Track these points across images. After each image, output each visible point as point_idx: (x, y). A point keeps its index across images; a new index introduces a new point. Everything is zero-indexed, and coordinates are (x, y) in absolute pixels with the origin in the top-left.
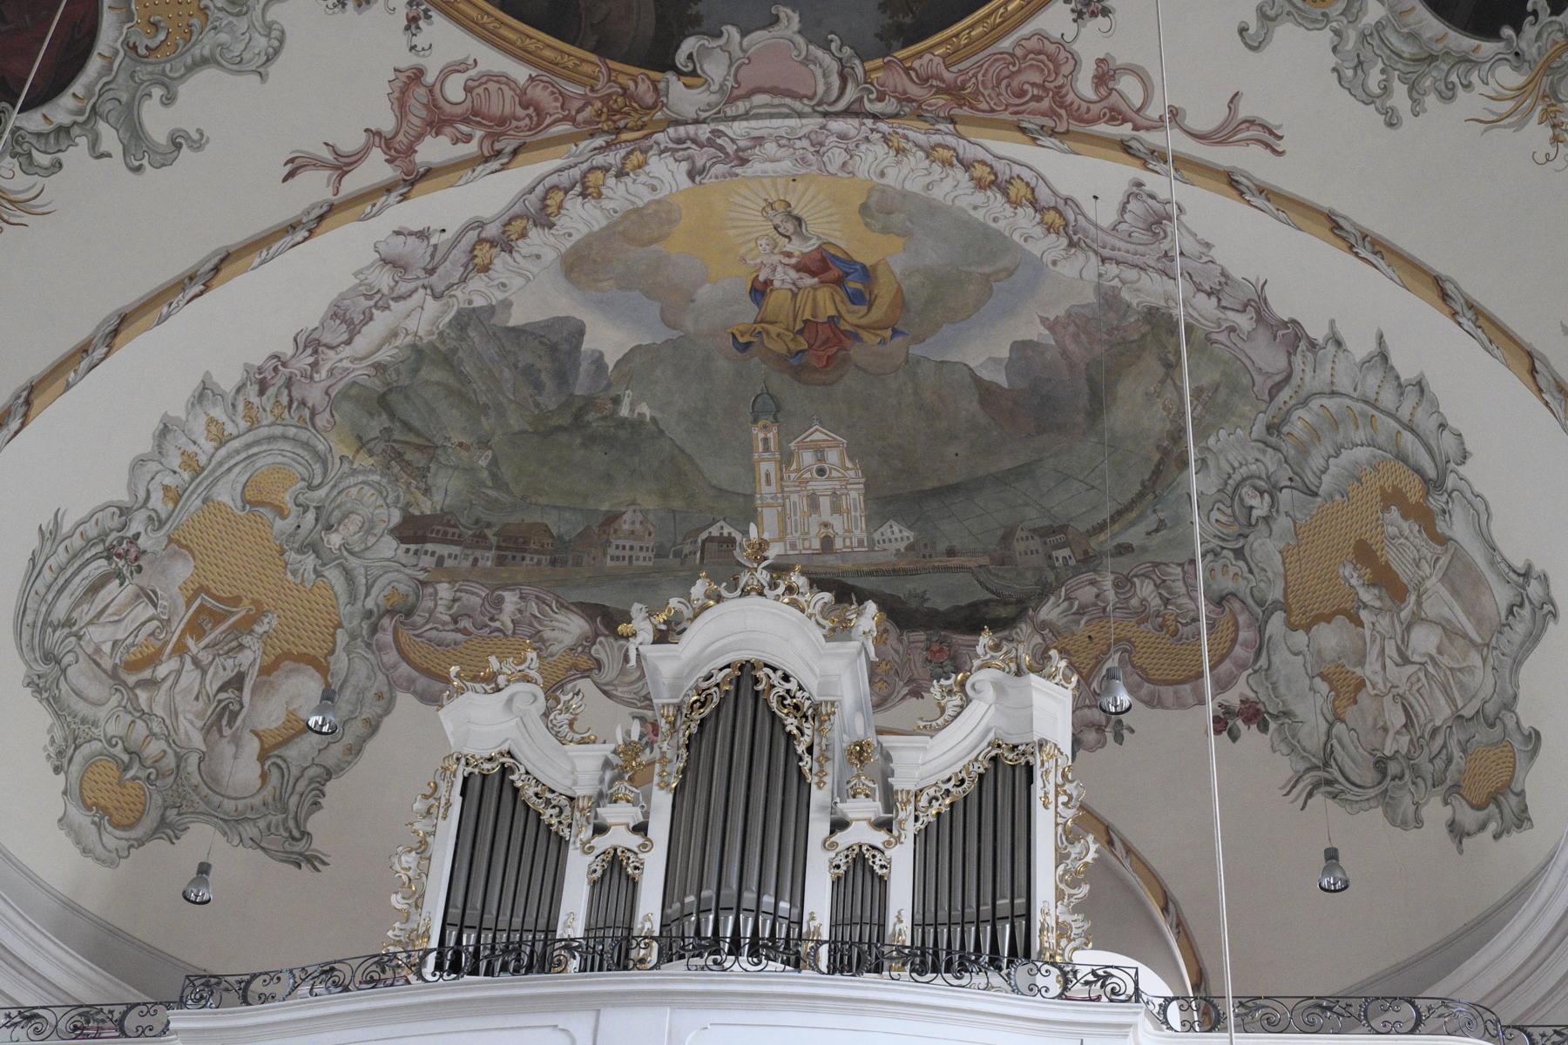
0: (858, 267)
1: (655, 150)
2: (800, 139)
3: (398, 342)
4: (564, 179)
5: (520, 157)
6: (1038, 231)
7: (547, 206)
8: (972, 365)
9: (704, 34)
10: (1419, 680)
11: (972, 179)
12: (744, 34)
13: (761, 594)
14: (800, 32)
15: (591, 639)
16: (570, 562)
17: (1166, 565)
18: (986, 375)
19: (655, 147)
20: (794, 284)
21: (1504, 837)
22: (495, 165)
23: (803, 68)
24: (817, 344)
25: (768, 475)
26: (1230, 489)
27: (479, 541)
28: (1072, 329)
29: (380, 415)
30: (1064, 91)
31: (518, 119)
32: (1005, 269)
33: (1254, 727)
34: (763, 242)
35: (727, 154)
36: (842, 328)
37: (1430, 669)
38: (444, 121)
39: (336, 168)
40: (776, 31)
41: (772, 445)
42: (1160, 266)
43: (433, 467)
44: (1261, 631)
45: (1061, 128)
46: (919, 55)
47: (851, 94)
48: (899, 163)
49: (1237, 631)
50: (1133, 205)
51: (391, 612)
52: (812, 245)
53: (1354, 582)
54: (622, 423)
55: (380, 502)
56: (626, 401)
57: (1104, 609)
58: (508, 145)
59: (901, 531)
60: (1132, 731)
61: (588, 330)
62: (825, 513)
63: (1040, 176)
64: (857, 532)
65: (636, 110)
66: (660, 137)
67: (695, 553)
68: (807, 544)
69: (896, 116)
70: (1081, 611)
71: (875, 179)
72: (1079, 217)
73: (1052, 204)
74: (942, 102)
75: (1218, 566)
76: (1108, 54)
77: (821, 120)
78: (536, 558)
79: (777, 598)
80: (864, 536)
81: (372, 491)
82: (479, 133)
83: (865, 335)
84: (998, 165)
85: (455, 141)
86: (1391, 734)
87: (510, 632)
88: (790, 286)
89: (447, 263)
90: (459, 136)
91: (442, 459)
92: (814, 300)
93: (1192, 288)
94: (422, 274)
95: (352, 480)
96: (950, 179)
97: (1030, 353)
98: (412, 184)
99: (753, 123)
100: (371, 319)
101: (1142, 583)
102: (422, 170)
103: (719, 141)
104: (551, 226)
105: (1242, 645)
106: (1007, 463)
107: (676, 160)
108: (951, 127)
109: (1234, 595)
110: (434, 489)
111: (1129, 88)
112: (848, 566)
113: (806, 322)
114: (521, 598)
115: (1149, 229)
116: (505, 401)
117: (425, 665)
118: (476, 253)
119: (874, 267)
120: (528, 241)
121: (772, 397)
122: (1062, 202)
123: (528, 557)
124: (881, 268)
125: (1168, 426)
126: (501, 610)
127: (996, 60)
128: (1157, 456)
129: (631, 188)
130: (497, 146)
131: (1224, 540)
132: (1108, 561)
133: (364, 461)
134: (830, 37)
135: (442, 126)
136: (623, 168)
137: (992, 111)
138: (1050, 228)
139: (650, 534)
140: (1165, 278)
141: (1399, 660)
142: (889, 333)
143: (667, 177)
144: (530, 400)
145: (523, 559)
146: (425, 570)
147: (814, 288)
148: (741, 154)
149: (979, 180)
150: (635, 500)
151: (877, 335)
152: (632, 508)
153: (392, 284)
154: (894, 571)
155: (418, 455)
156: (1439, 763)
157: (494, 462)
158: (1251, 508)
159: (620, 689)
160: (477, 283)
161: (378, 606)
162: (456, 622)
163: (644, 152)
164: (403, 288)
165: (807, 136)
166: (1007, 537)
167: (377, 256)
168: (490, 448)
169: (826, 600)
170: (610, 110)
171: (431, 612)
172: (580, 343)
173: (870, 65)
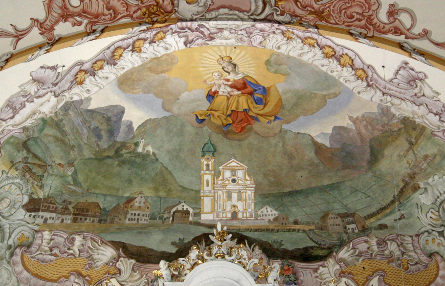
0: (261, 88)
1: (170, 32)
2: (241, 30)
3: (36, 117)
4: (124, 44)
5: (105, 34)
6: (353, 78)
7: (114, 55)
8: (313, 135)
11: (323, 53)
13: (223, 258)
16: (108, 221)
17: (404, 236)
18: (319, 140)
19: (170, 31)
20: (229, 93)
22: (92, 37)
24: (237, 121)
25: (207, 182)
26: (438, 203)
27: (65, 211)
28: (364, 123)
29: (23, 151)
30: (372, 17)
31: (105, 15)
32: (335, 93)
34: (216, 74)
39: (16, 36)
42: (412, 99)
43: (46, 175)
45: (370, 35)
47: (268, 11)
48: (288, 43)
50: (402, 72)
51: (20, 246)
52: (240, 76)
54: (139, 155)
55: (19, 192)
56: (141, 145)
57: (372, 255)
58: (100, 27)
59: (271, 211)
61: (126, 111)
63: (357, 55)
64: (250, 210)
65: (162, 13)
66: (173, 26)
67: (169, 218)
68: (224, 215)
69: (289, 23)
70: (360, 255)
71: (275, 50)
72: (374, 75)
73: (361, 67)
74: (312, 18)
75: (430, 239)
76: (395, 2)
77: (252, 23)
78: (92, 219)
79: (232, 261)
80: (253, 212)
81: (16, 187)
82: (85, 21)
83: (261, 118)
84: (337, 49)
85: (74, 25)
87: (77, 256)
88: (227, 94)
89: (63, 81)
90: (76, 22)
91: (51, 172)
92: (238, 101)
93: (427, 111)
94: (51, 86)
95: (7, 182)
96: (312, 53)
97: (342, 132)
98: (52, 45)
99: (219, 22)
100: (24, 107)
101: (391, 243)
102: (57, 38)
103: (201, 29)
104: (115, 64)
105: (440, 277)
106: (326, 182)
107: (179, 37)
108: (316, 30)
109: (437, 253)
110: (45, 186)
111: (405, 19)
112: (245, 226)
113: (233, 111)
114: (84, 238)
115: (409, 83)
116: (82, 143)
117: (36, 272)
118: (78, 76)
119: (269, 88)
120: (103, 71)
121: (213, 145)
122: (367, 67)
123: (88, 218)
125: (409, 171)
126: (73, 245)
128: (402, 185)
129: (156, 48)
130: (94, 28)
132: (373, 231)
133: (13, 173)
135: (68, 18)
136: (153, 39)
137: (337, 24)
138: (358, 78)
139: (148, 208)
140: (414, 105)
142: (273, 118)
143: (174, 44)
144: (95, 143)
145: (86, 219)
146: (37, 225)
147: (238, 96)
148: (211, 35)
149: (327, 54)
150: (142, 192)
151: (268, 119)
152: (140, 196)
153: (36, 90)
154: (267, 230)
155: (39, 169)
157: (75, 172)
160: (76, 90)
161: (14, 242)
162: (51, 250)
163: (165, 33)
164: (41, 92)
165: (244, 29)
166: (325, 216)
167: (31, 78)
168: (73, 166)
169: (255, 262)
170: (150, 12)
171: (40, 246)
172: (122, 117)
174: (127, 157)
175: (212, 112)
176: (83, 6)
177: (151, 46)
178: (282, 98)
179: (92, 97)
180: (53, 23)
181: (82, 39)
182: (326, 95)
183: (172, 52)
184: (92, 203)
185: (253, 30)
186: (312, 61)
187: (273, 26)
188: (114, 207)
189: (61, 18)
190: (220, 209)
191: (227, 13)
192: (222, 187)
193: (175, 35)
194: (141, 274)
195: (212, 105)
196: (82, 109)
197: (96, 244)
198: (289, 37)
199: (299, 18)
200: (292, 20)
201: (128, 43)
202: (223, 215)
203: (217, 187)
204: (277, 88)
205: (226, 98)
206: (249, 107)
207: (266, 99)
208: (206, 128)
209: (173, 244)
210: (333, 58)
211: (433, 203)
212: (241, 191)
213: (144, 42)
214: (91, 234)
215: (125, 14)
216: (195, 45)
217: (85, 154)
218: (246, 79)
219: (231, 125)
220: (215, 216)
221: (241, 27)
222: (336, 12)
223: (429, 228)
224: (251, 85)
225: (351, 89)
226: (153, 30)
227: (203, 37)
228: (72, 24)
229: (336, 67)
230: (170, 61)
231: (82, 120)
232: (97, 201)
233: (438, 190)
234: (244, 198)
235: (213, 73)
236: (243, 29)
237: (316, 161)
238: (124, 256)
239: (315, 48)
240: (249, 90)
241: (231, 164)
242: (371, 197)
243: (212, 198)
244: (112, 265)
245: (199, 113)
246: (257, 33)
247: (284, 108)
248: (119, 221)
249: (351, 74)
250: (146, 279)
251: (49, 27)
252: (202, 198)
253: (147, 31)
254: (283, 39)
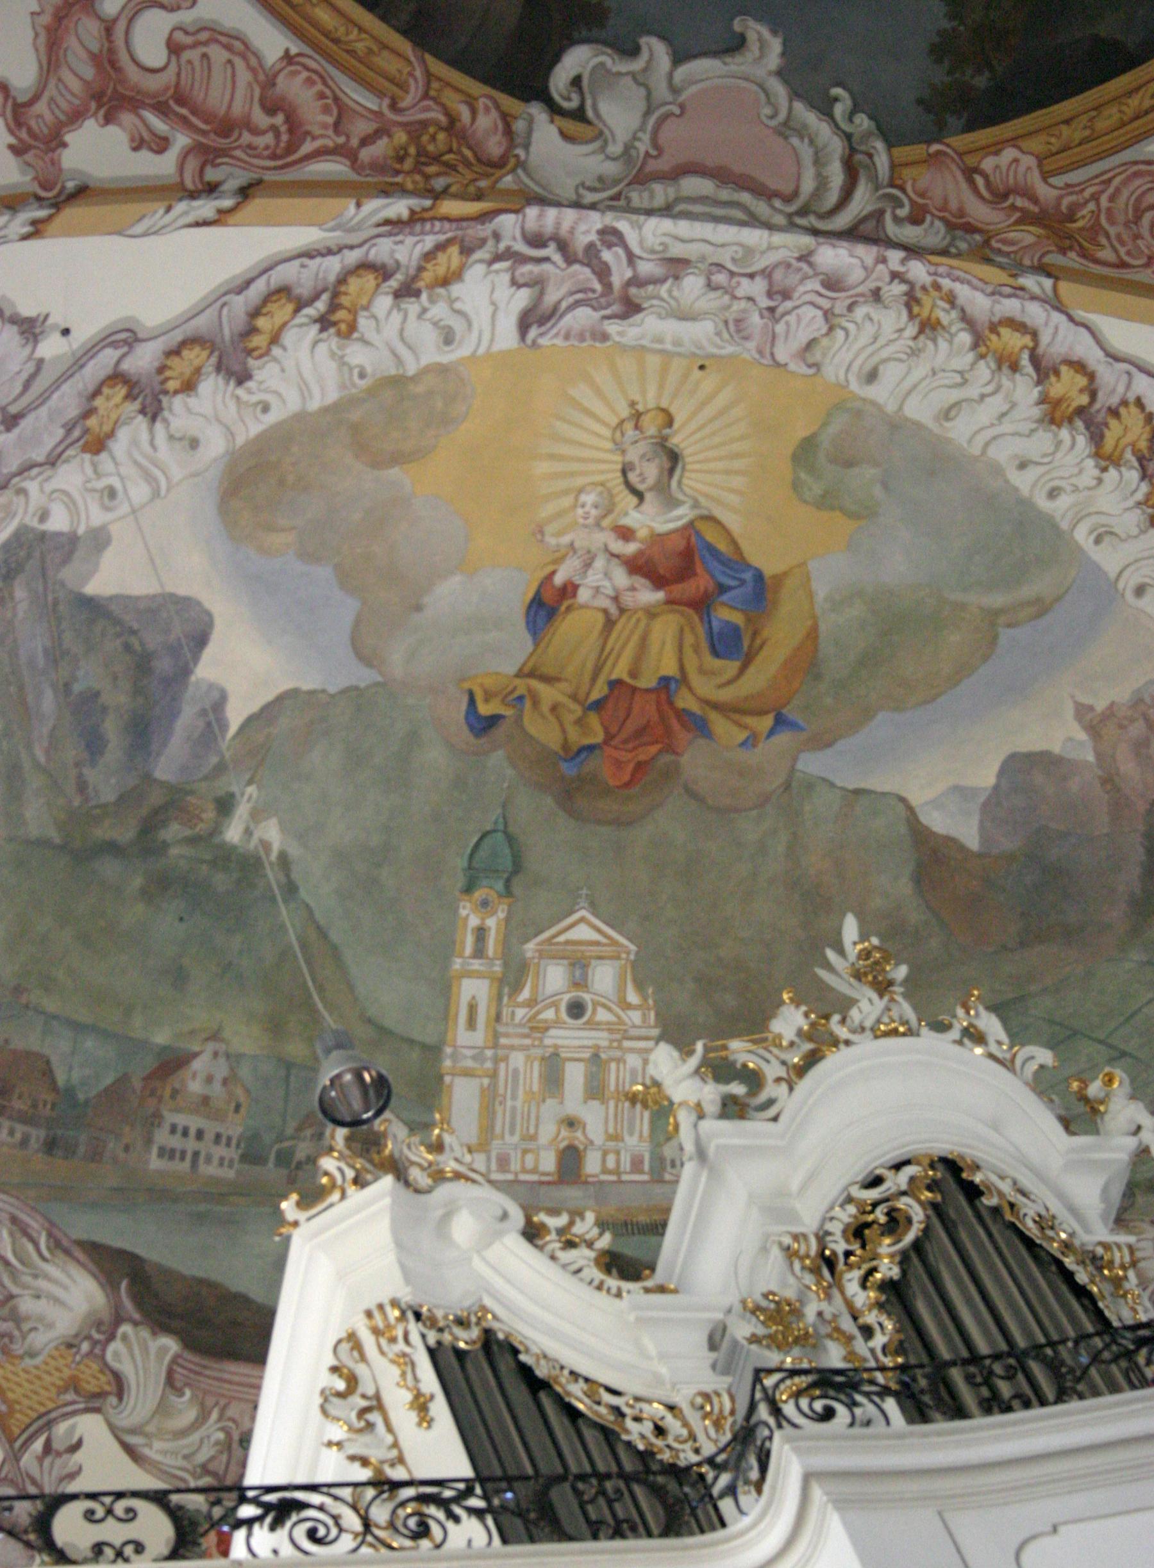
2: (751, 276)
5: (257, 204)
8: (916, 798)
9: (604, 43)
11: (1043, 400)
12: (678, 59)
14: (779, 73)
16: (82, 1149)
18: (937, 822)
20: (616, 599)
22: (206, 208)
23: (780, 140)
25: (472, 1008)
28: (1138, 729)
31: (256, 132)
32: (1038, 600)
34: (589, 498)
35: (608, 286)
36: (680, 704)
38: (123, 97)
40: (737, 64)
41: (492, 945)
46: (995, 148)
47: (862, 201)
48: (914, 353)
52: (683, 514)
54: (225, 857)
56: (242, 811)
58: (232, 177)
62: (574, 1097)
65: (468, 165)
66: (507, 223)
68: (530, 1164)
71: (854, 386)
74: (1030, 239)
77: (807, 240)
78: (20, 1129)
80: (645, 1150)
82: (181, 140)
83: (720, 725)
85: (138, 144)
89: (43, 411)
92: (644, 639)
98: (57, 205)
99: (683, 227)
102: (70, 185)
103: (607, 255)
108: (1048, 283)
113: (615, 684)
116: (27, 765)
118: (99, 402)
119: (779, 579)
120: (192, 401)
121: (510, 839)
124: (790, 584)
127: (1136, 175)
130: (211, 175)
134: (837, 91)
136: (415, 278)
137: (1123, 265)
139: (237, 1108)
142: (768, 721)
144: (74, 772)
147: (651, 613)
148: (633, 291)
149: (1058, 403)
150: (220, 1029)
151: (746, 727)
152: (211, 1047)
159: (157, 1445)
165: (767, 273)
170: (421, 152)
173: (904, 152)
174: (182, 863)
175: (534, 683)
176: (179, 74)
177: (399, 310)
178: (822, 627)
179: (114, 529)
180: (62, 117)
181: (169, 209)
182: (995, 613)
183: (461, 361)
184: (28, 1054)
185: (798, 277)
186: (987, 445)
187: (884, 261)
188: (106, 1090)
189: (93, 105)
190: (512, 1133)
191: (707, 197)
192: (527, 1036)
193: (497, 272)
194: (202, 1405)
195: (539, 651)
196: (62, 584)
197: (30, 1247)
198: (929, 319)
199: (978, 237)
200: (951, 244)
201: (321, 275)
202: (523, 1162)
203: (507, 1035)
204: (809, 579)
205: (601, 618)
206: (682, 668)
207: (755, 634)
208: (498, 757)
210: (1079, 424)
212: (603, 1056)
213: (378, 286)
214: (12, 1200)
215: (331, 144)
216: (557, 335)
217: (28, 814)
218: (698, 533)
219: (597, 752)
220: (494, 1166)
221: (758, 256)
222: (1121, 218)
224: (714, 565)
225: (1112, 575)
226: (428, 226)
227: (602, 295)
228: (132, 140)
229: (1076, 470)
230: (440, 404)
231: (49, 644)
232: (47, 1051)
234: (612, 1087)
235: (580, 491)
236: (763, 271)
237: (915, 915)
238: (137, 1316)
239: (1017, 376)
240: (698, 588)
241: (573, 935)
242: (1130, 1055)
243: (486, 1081)
244: (90, 1354)
245: (482, 685)
246: (807, 298)
247: (818, 677)
248: (122, 1155)
249: (1130, 503)
250: (222, 1429)
251: (46, 131)
252: (447, 1079)
253: (407, 230)
254: (901, 330)
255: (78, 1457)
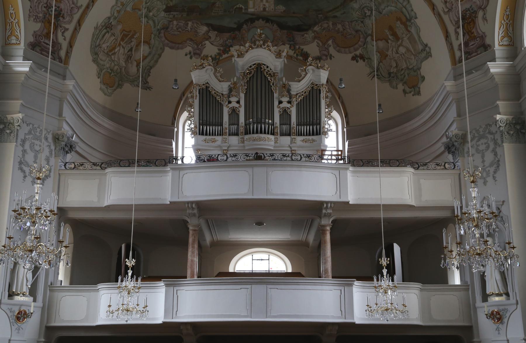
10: (400, 58)
13: (261, 46)
15: (208, 32)
21: (415, 96)
33: (362, 60)
37: (403, 56)
44: (366, 39)
49: (360, 39)
53: (388, 34)
57: (329, 30)
60: (334, 57)
67: (233, 11)
68: (259, 9)
70: (324, 29)
79: (265, 48)
86: (393, 67)
87: (190, 31)
109: (360, 31)
126: (188, 26)
131: (359, 18)
141: (396, 52)
145: (193, 14)
146: (170, 18)
156: (402, 76)
158: (366, 13)
161: (160, 27)
171: (172, 28)
209: (235, 23)
211: (359, 8)
223: (357, 19)
233: (362, 2)
238: (211, 30)
255: (206, 45)
